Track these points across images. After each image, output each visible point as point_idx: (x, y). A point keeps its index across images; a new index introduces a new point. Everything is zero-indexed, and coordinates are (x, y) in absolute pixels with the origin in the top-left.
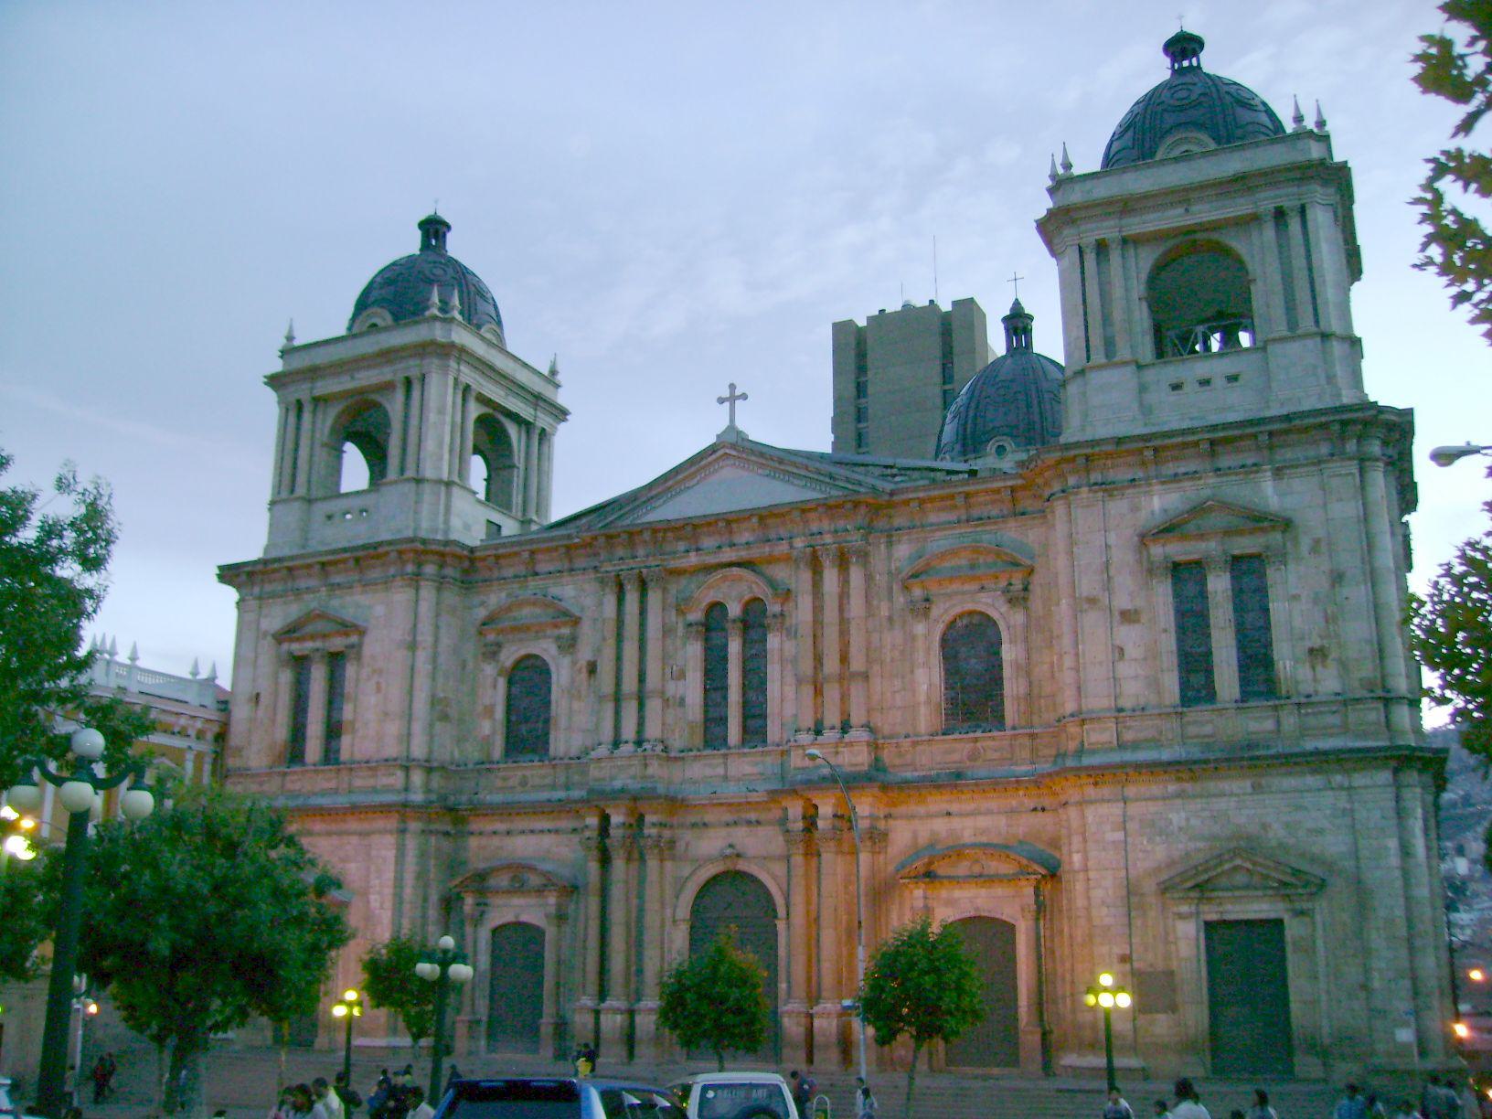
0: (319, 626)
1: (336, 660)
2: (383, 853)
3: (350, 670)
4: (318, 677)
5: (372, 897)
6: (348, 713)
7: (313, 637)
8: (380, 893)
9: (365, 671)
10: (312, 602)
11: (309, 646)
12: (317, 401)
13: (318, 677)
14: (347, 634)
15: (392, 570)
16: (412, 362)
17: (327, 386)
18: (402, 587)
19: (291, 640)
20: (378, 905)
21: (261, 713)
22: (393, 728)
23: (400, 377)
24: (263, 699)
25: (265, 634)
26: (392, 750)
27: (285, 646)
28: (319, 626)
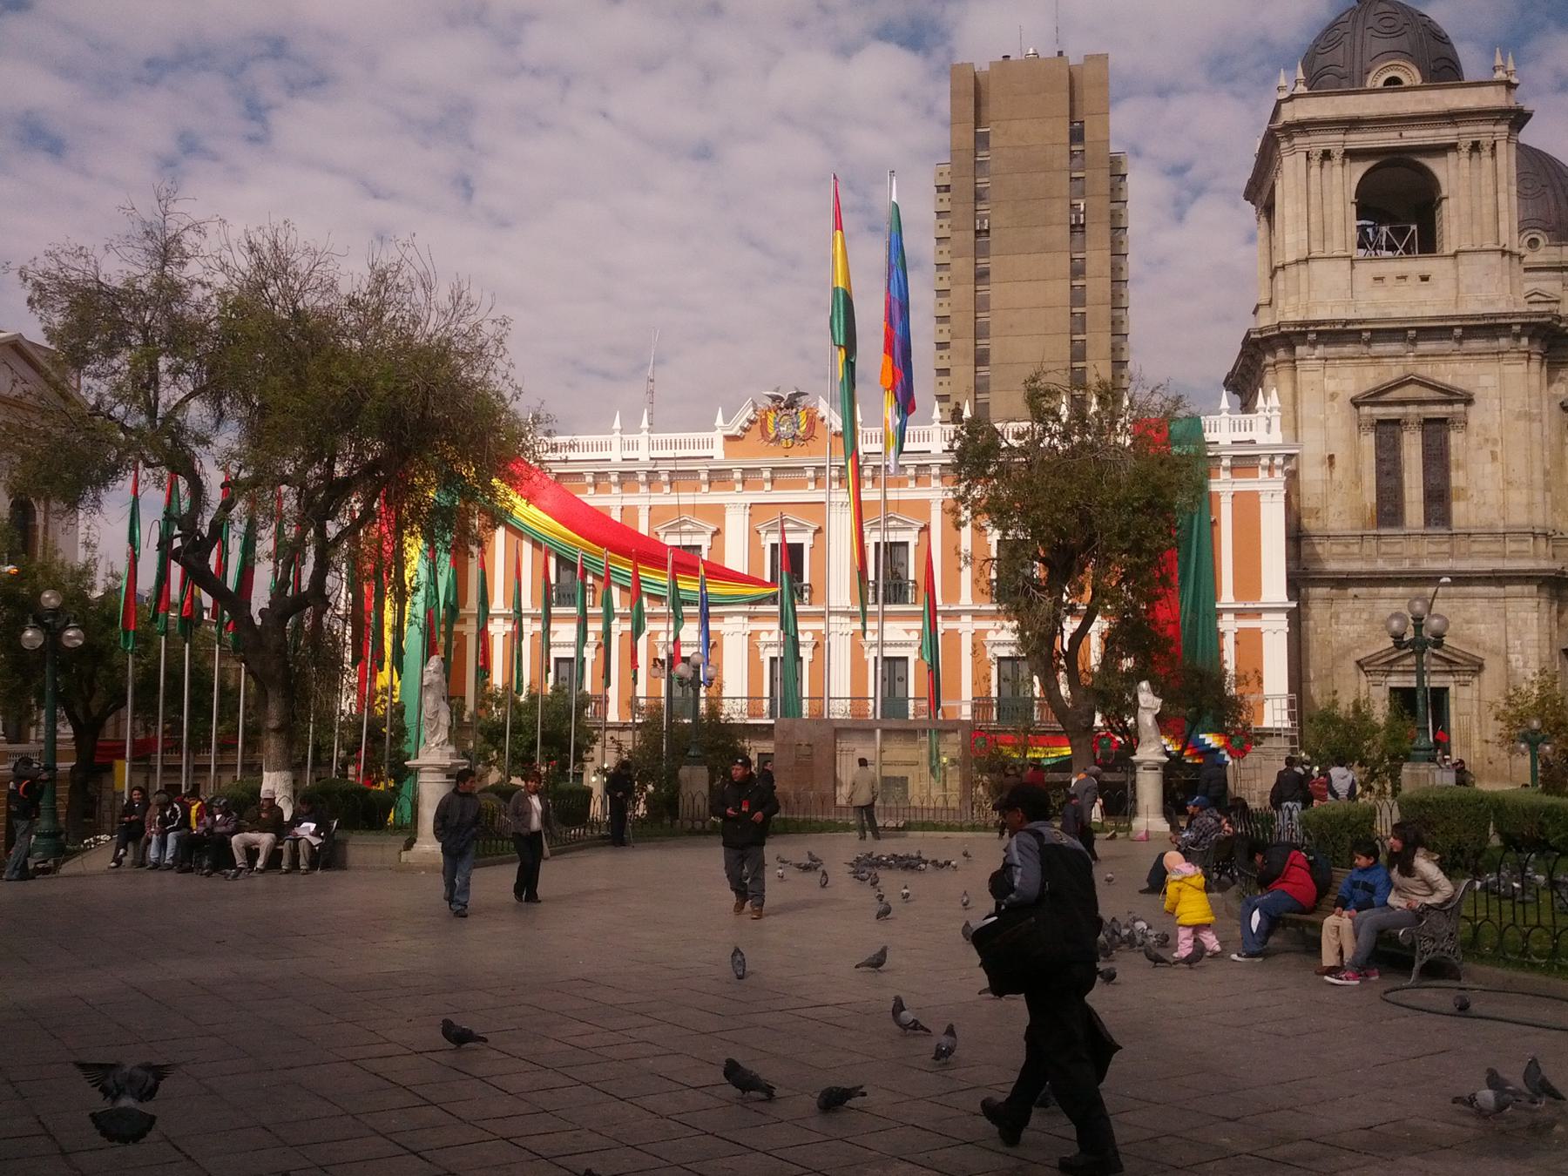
0: (1411, 391)
1: (1436, 431)
2: (1523, 615)
3: (1455, 438)
4: (1412, 448)
5: (1512, 657)
6: (1457, 479)
7: (1403, 403)
8: (1522, 653)
9: (1473, 441)
10: (1395, 371)
11: (1395, 412)
12: (1352, 155)
13: (1412, 448)
14: (1450, 402)
15: (1503, 342)
16: (1482, 128)
17: (1358, 140)
18: (1517, 358)
19: (1374, 404)
20: (1521, 664)
21: (1338, 473)
22: (1518, 497)
23: (1465, 143)
24: (1337, 460)
25: (1333, 396)
26: (1519, 518)
27: (1366, 410)
28: (1411, 391)
